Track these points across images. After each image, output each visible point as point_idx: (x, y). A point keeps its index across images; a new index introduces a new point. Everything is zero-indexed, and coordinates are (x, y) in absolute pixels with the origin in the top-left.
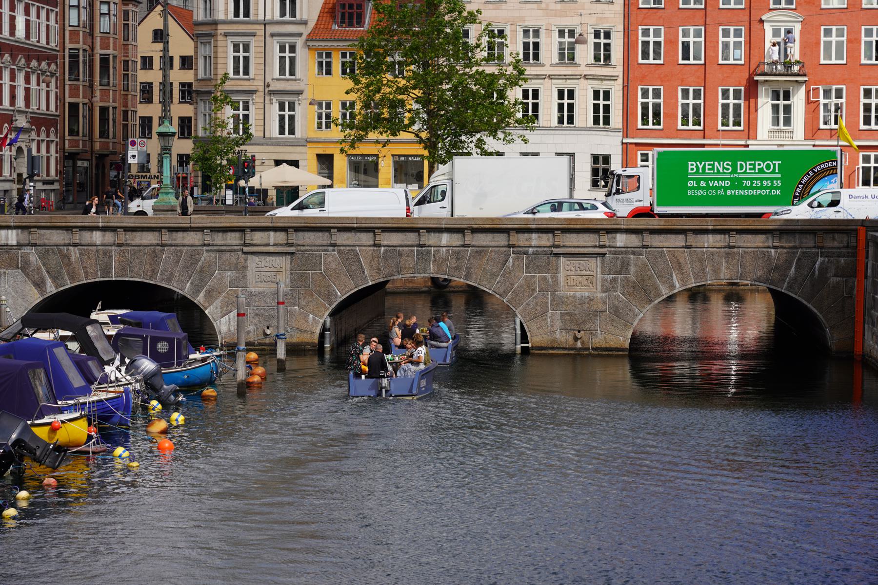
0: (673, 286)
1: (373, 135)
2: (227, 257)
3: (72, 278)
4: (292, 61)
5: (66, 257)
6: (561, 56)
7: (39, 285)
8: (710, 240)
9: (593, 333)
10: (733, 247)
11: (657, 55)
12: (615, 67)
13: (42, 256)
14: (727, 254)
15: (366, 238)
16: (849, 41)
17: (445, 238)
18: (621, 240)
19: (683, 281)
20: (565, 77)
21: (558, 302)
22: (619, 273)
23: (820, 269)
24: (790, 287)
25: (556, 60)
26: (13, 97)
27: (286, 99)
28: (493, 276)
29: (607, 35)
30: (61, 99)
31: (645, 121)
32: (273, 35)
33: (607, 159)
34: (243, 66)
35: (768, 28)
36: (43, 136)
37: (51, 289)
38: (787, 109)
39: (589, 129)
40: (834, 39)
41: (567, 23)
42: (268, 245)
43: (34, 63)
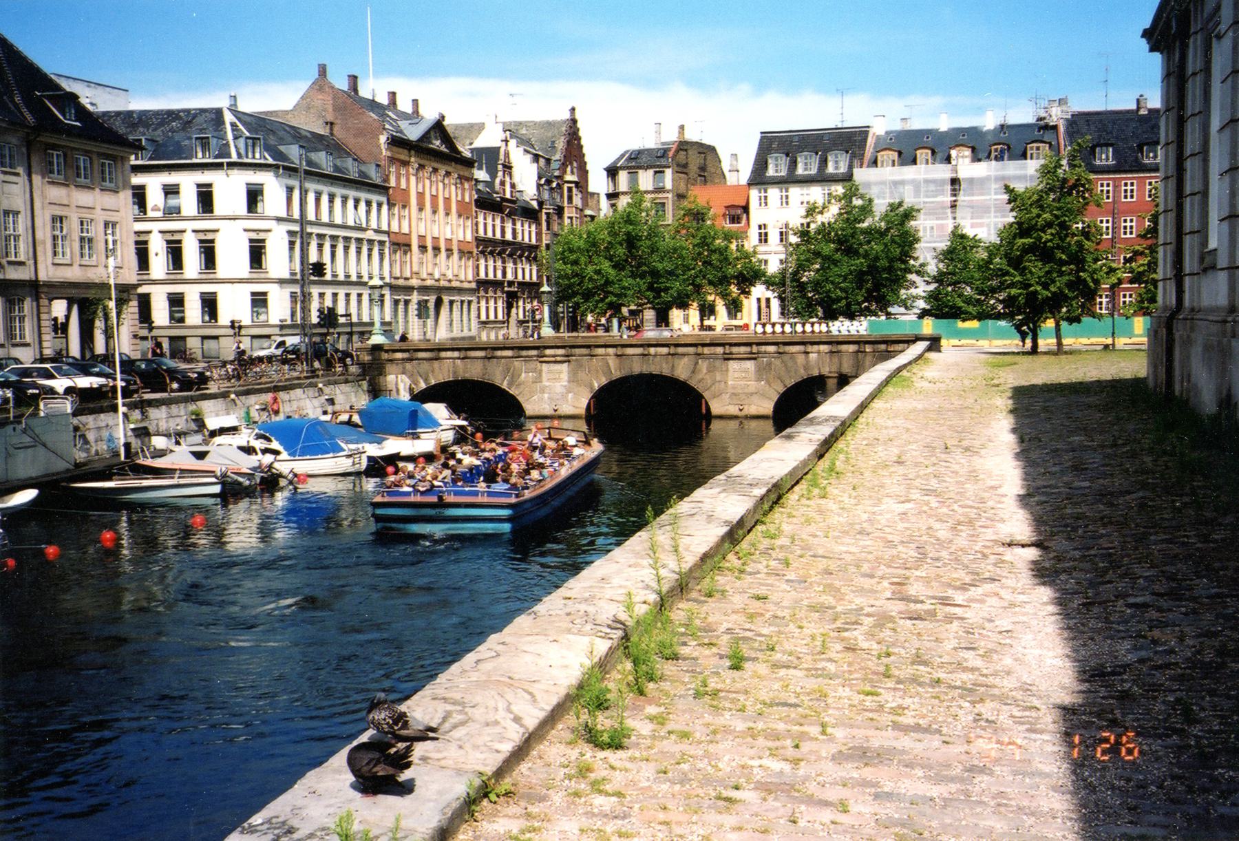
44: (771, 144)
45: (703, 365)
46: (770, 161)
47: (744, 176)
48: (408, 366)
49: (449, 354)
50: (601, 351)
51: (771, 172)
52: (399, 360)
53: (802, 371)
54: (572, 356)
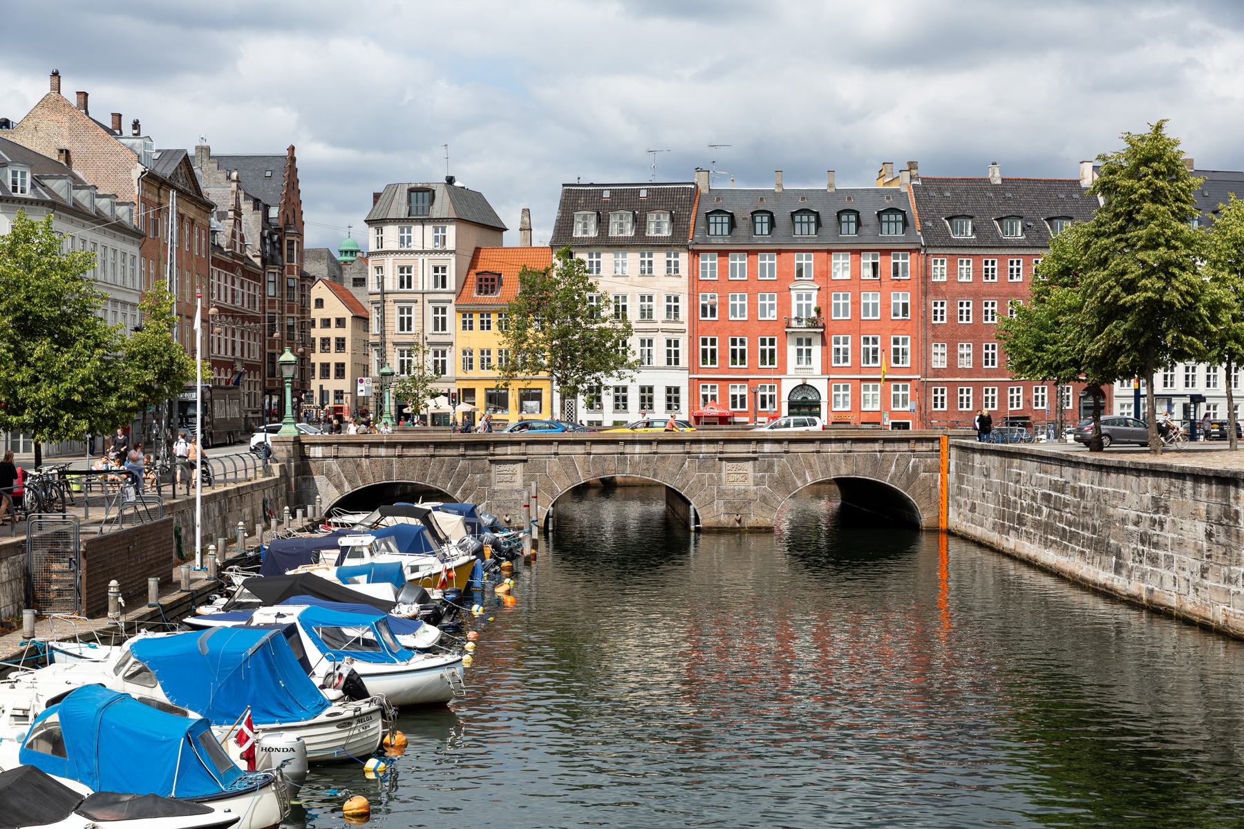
0: (805, 481)
1: (520, 375)
2: (479, 464)
3: (364, 481)
4: (444, 320)
5: (358, 465)
6: (643, 315)
7: (338, 486)
8: (833, 447)
9: (747, 515)
10: (850, 452)
11: (713, 314)
12: (683, 323)
13: (341, 465)
14: (845, 456)
15: (579, 449)
16: (853, 303)
17: (638, 448)
18: (767, 448)
19: (813, 476)
20: (646, 331)
21: (721, 494)
22: (766, 471)
23: (913, 467)
24: (892, 479)
25: (638, 317)
26: (234, 349)
27: (440, 348)
28: (674, 475)
29: (676, 300)
30: (263, 350)
31: (704, 362)
32: (430, 302)
33: (677, 390)
34: (405, 324)
35: (794, 294)
36: (252, 378)
37: (348, 489)
38: (809, 352)
39: (664, 368)
40: (841, 301)
41: (646, 291)
42: (506, 455)
43: (246, 324)
46: (577, 219)
47: (543, 235)
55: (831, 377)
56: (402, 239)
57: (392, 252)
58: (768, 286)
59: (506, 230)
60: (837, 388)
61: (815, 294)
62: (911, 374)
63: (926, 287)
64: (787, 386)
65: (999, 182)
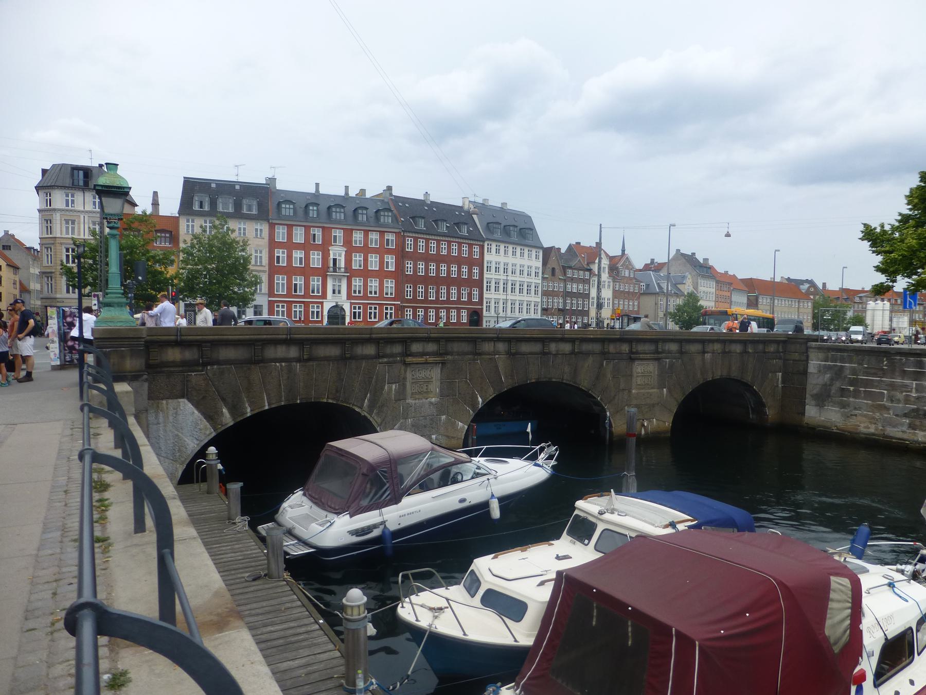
29: (261, 252)
37: (227, 419)
44: (192, 188)
45: (608, 367)
48: (195, 378)
49: (281, 351)
50: (487, 347)
51: (196, 207)
52: (174, 364)
53: (699, 375)
54: (447, 354)
55: (352, 301)
56: (67, 201)
57: (59, 210)
58: (316, 248)
59: (137, 206)
60: (355, 308)
61: (343, 254)
62: (395, 301)
63: (401, 255)
64: (327, 306)
65: (430, 203)
